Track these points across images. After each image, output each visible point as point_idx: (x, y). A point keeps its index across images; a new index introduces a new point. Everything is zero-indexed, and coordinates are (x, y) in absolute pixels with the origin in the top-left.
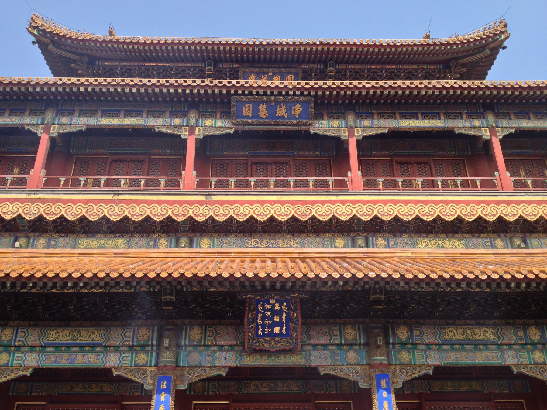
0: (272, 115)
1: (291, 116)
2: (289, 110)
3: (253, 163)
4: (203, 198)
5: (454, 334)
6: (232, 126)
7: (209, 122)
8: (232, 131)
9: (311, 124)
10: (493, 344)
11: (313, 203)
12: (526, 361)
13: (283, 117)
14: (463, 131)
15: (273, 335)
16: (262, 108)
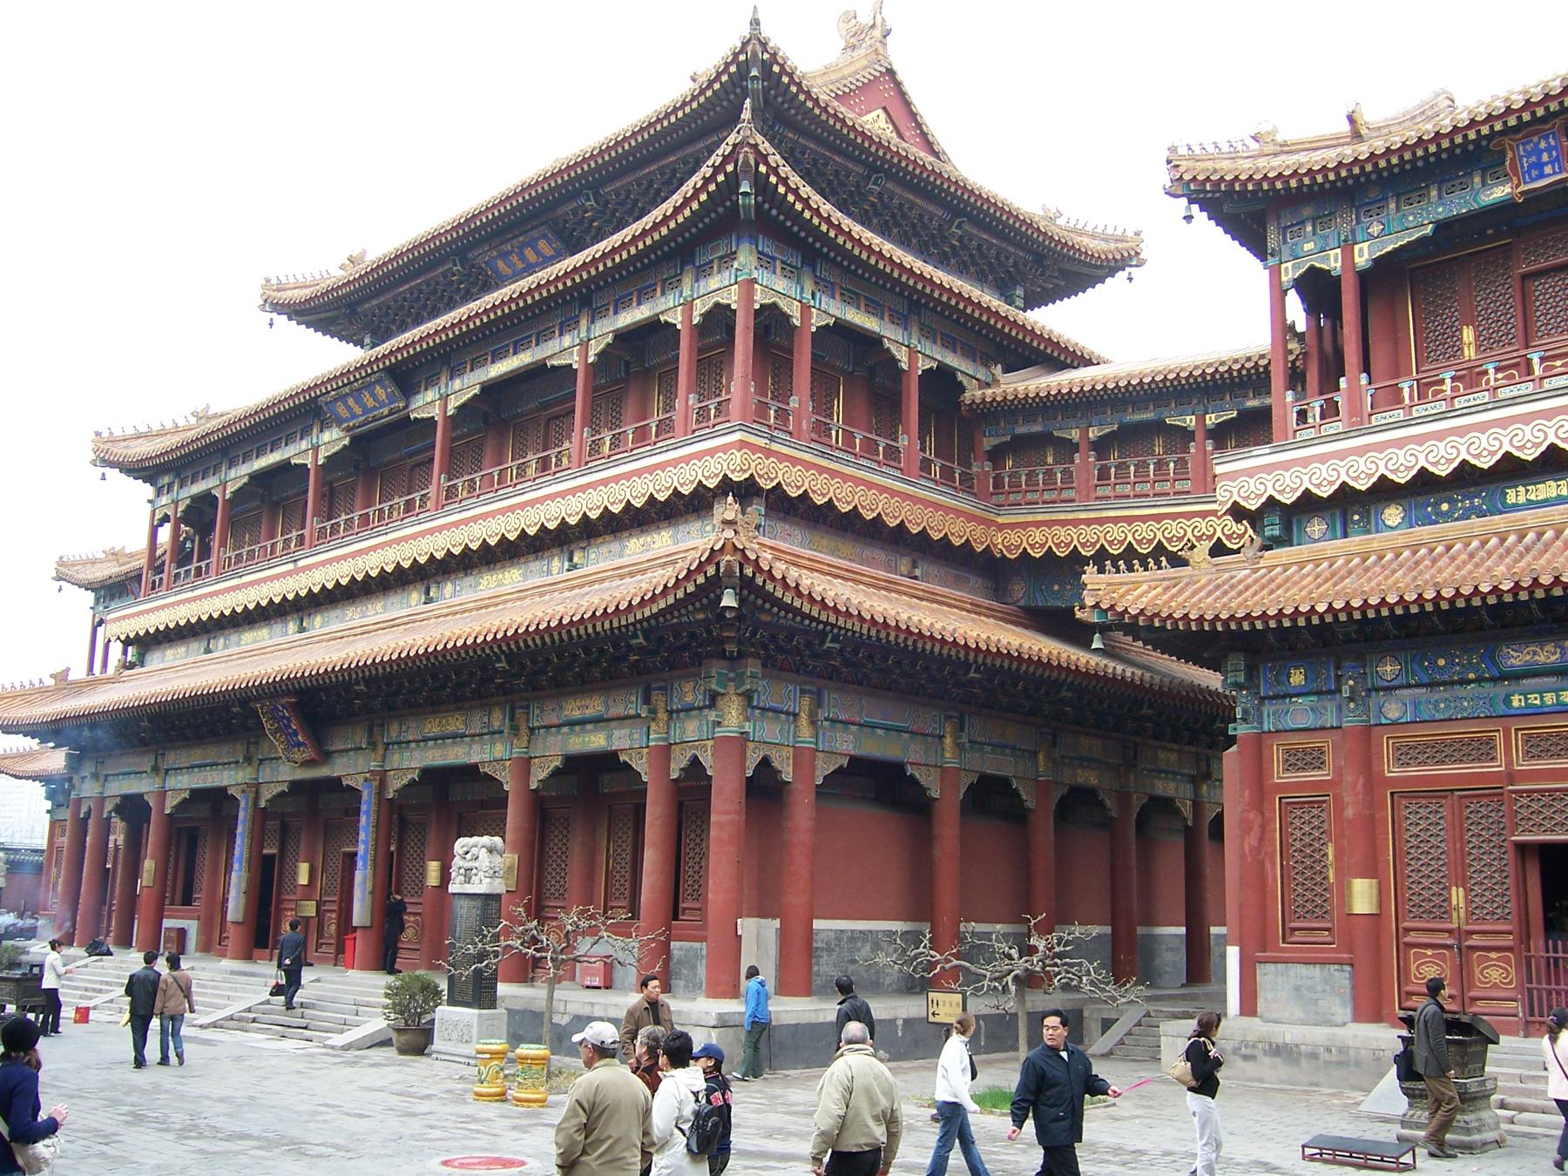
0: (366, 411)
1: (381, 403)
2: (373, 395)
3: (414, 466)
4: (290, 566)
5: (432, 727)
6: (342, 434)
7: (326, 436)
8: (346, 442)
9: (406, 407)
10: (463, 736)
11: (366, 551)
12: (486, 757)
13: (374, 408)
14: (555, 363)
15: (299, 744)
16: (351, 401)
